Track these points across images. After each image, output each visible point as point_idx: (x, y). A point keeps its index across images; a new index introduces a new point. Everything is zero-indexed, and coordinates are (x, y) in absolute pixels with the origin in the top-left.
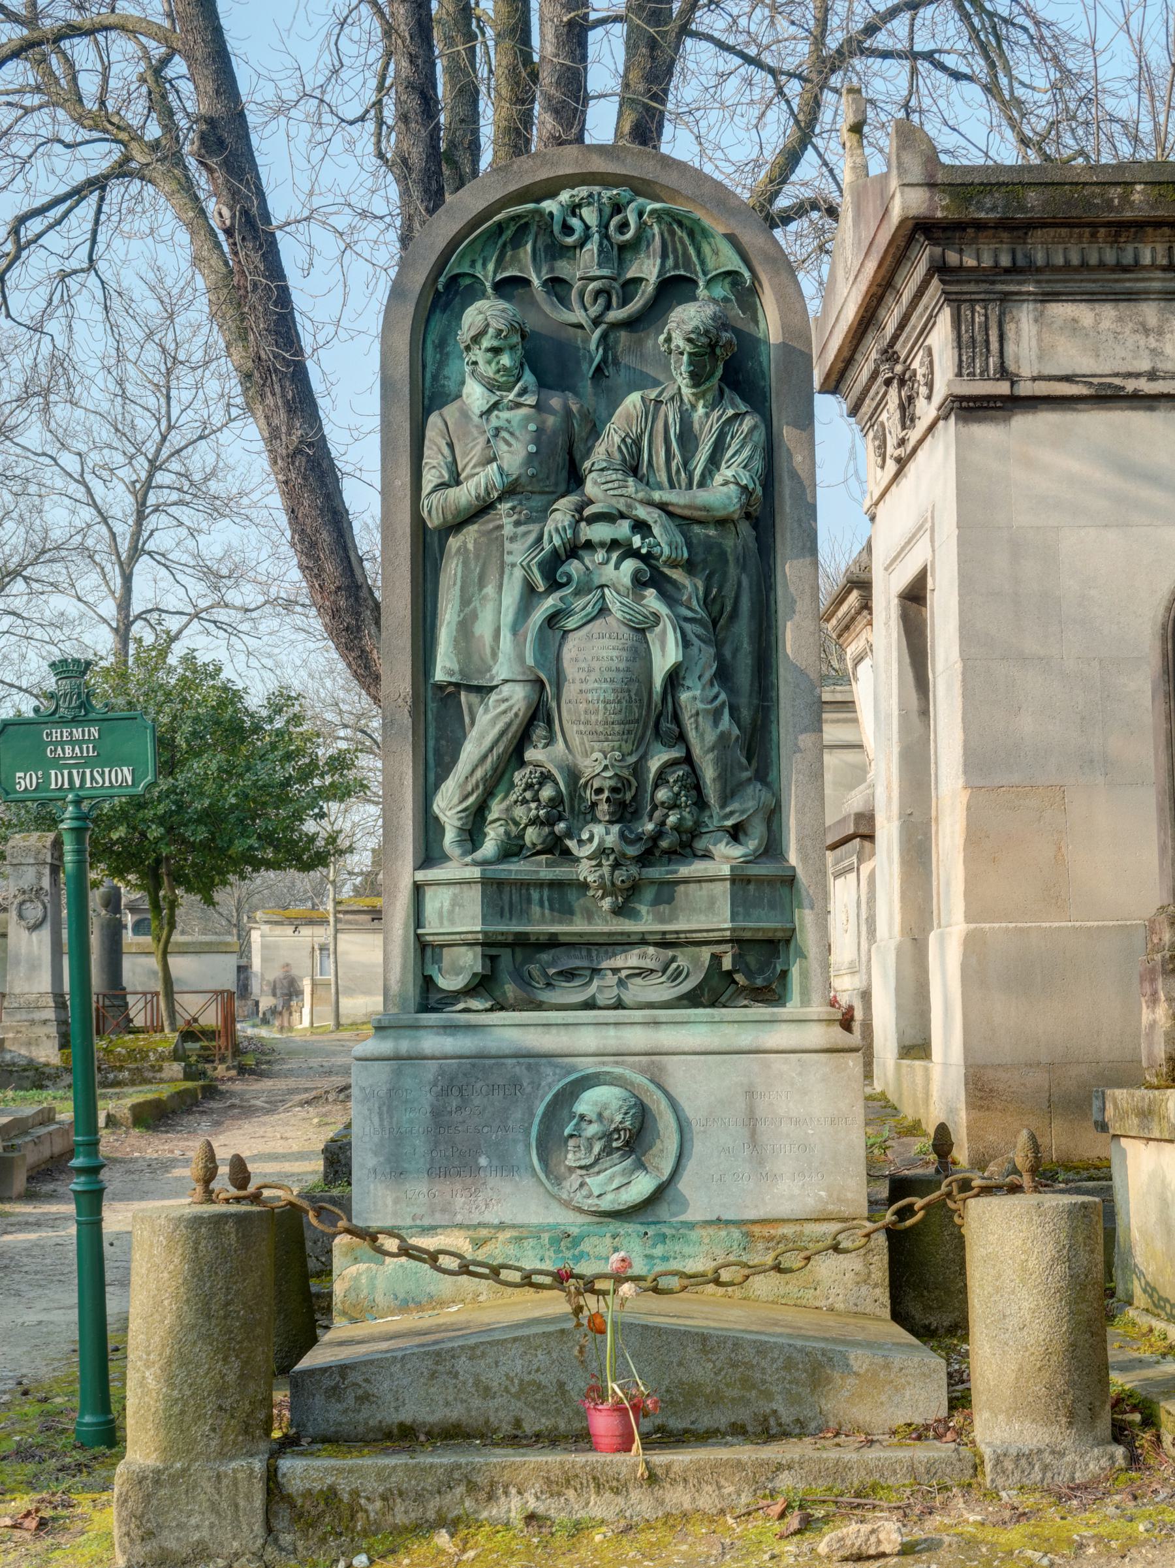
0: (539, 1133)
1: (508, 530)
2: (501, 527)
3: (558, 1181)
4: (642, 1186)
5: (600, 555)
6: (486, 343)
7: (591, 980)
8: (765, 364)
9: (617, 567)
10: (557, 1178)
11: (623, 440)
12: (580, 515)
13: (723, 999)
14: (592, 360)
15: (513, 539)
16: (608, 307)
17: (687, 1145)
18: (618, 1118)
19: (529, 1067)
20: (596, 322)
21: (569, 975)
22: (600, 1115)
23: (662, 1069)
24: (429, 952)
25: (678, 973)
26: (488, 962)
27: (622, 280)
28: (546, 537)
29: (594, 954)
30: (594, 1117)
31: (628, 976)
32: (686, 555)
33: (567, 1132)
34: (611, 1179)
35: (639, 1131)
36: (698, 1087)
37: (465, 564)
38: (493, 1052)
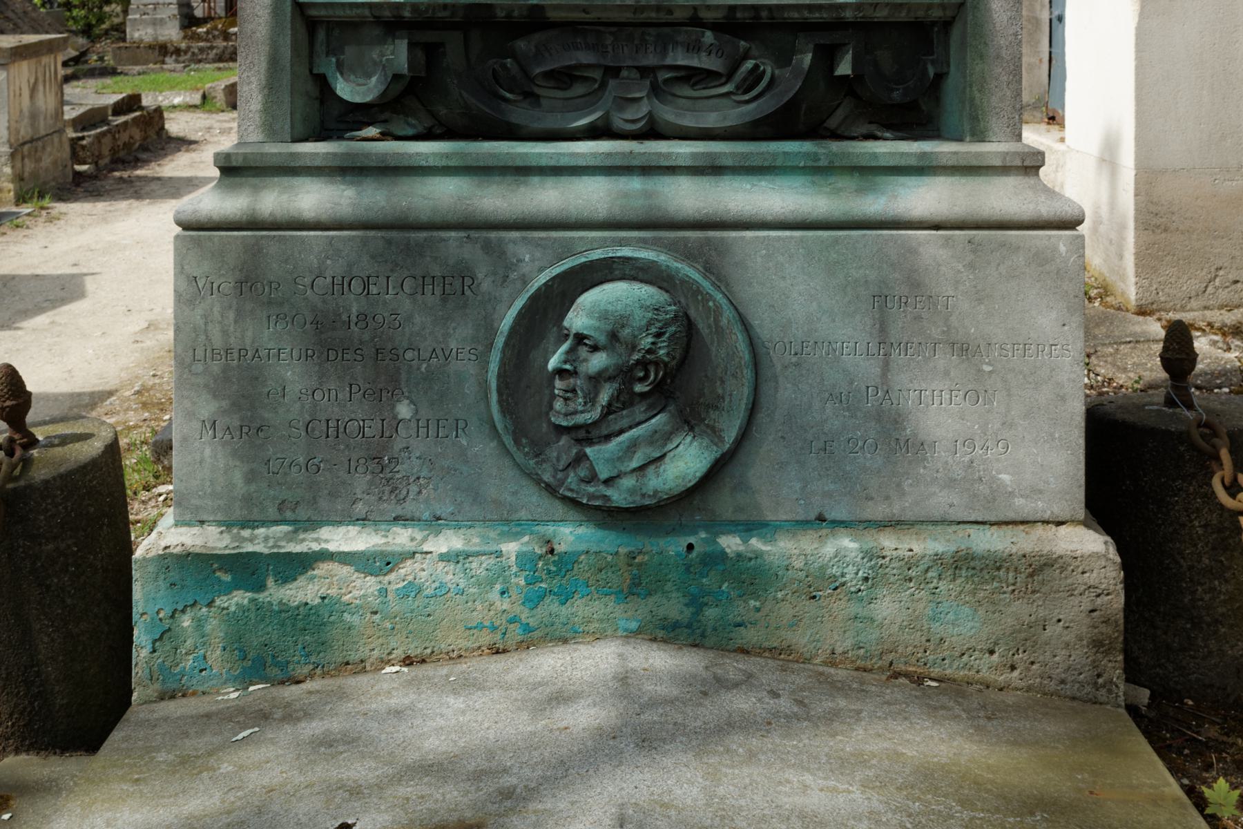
0: (503, 364)
3: (538, 450)
4: (687, 461)
7: (603, 85)
10: (533, 443)
13: (832, 123)
17: (766, 388)
18: (646, 342)
19: (487, 247)
21: (564, 77)
22: (613, 336)
23: (722, 249)
24: (321, 35)
25: (756, 76)
26: (420, 54)
29: (609, 40)
30: (602, 339)
31: (666, 81)
33: (553, 363)
34: (633, 446)
35: (683, 362)
36: (789, 293)
38: (424, 217)
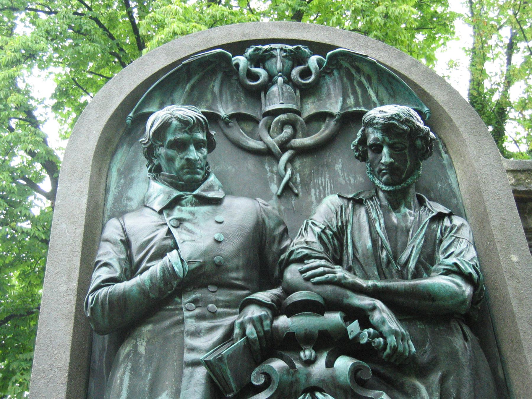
1: (191, 324)
2: (182, 322)
5: (307, 353)
6: (170, 138)
8: (454, 185)
9: (330, 364)
11: (323, 231)
12: (277, 308)
14: (281, 178)
15: (196, 334)
16: (294, 136)
20: (284, 146)
27: (305, 115)
28: (237, 331)
32: (413, 349)
37: (135, 371)
